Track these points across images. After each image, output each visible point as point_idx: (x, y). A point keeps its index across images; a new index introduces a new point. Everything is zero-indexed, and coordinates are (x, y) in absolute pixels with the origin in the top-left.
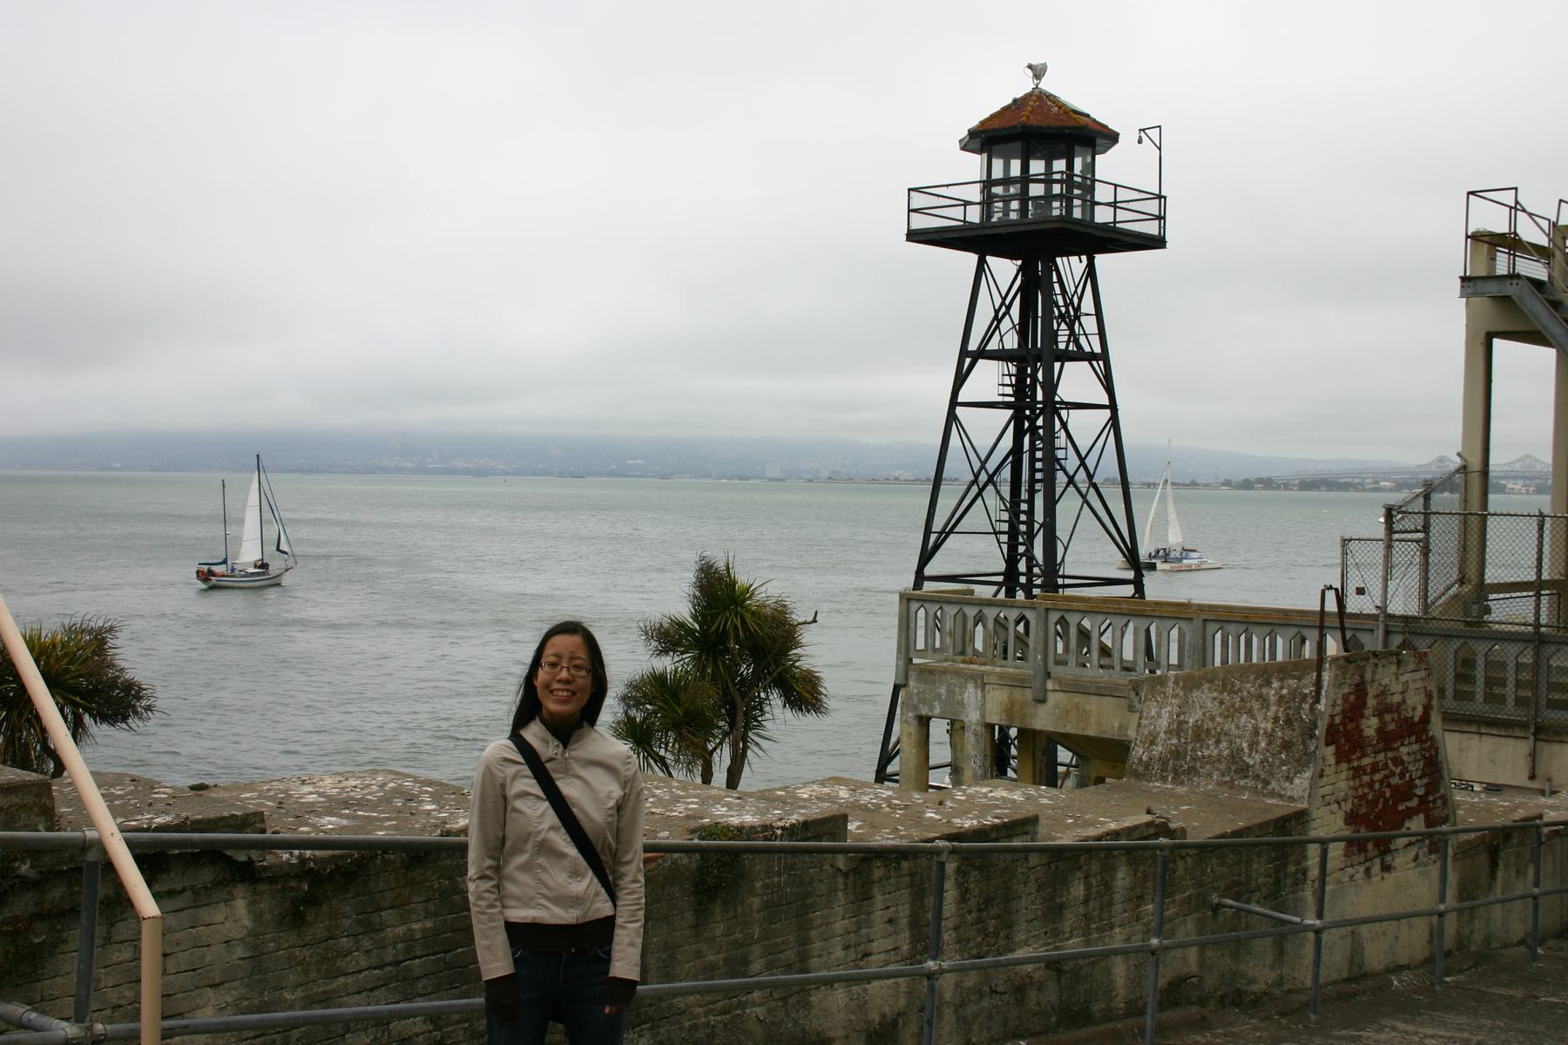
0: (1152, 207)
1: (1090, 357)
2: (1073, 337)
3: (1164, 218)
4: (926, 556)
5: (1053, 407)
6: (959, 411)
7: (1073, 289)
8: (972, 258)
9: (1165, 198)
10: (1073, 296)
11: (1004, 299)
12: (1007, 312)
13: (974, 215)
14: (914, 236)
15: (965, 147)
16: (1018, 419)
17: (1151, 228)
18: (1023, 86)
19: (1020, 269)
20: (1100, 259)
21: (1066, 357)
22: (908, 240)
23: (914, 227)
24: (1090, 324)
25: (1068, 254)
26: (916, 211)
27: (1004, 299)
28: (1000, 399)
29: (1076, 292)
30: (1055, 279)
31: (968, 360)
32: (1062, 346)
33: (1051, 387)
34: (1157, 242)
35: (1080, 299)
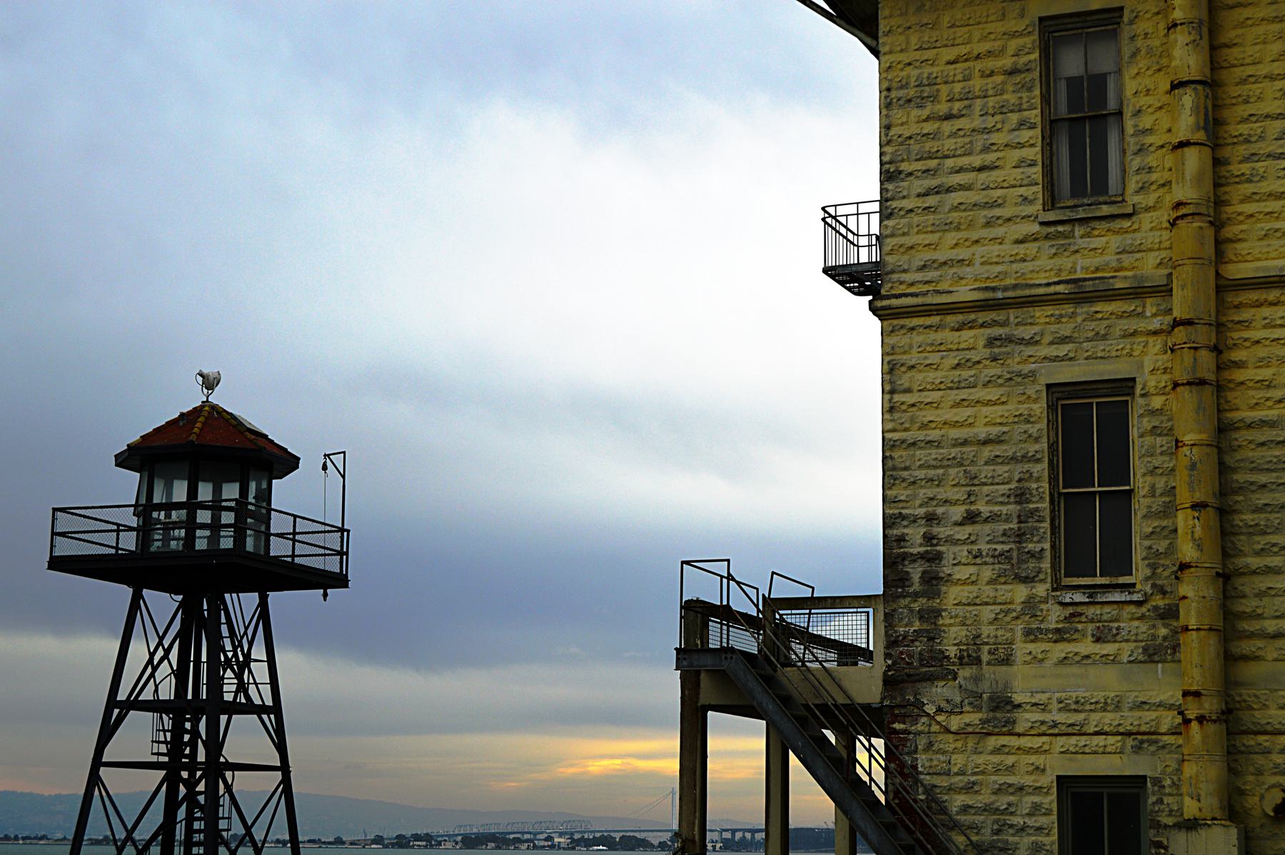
0: (333, 541)
1: (260, 710)
2: (242, 687)
3: (347, 554)
5: (217, 768)
6: (103, 772)
7: (242, 631)
8: (126, 592)
9: (348, 531)
10: (242, 638)
11: (161, 639)
12: (166, 656)
13: (129, 542)
14: (58, 563)
15: (124, 460)
16: (172, 780)
17: (332, 565)
18: (193, 398)
19: (182, 605)
20: (273, 597)
21: (234, 709)
22: (50, 568)
23: (56, 554)
24: (260, 671)
25: (238, 590)
26: (63, 534)
27: (161, 639)
28: (154, 759)
29: (246, 633)
30: (223, 620)
31: (116, 711)
32: (228, 697)
33: (215, 745)
34: (340, 580)
35: (251, 644)
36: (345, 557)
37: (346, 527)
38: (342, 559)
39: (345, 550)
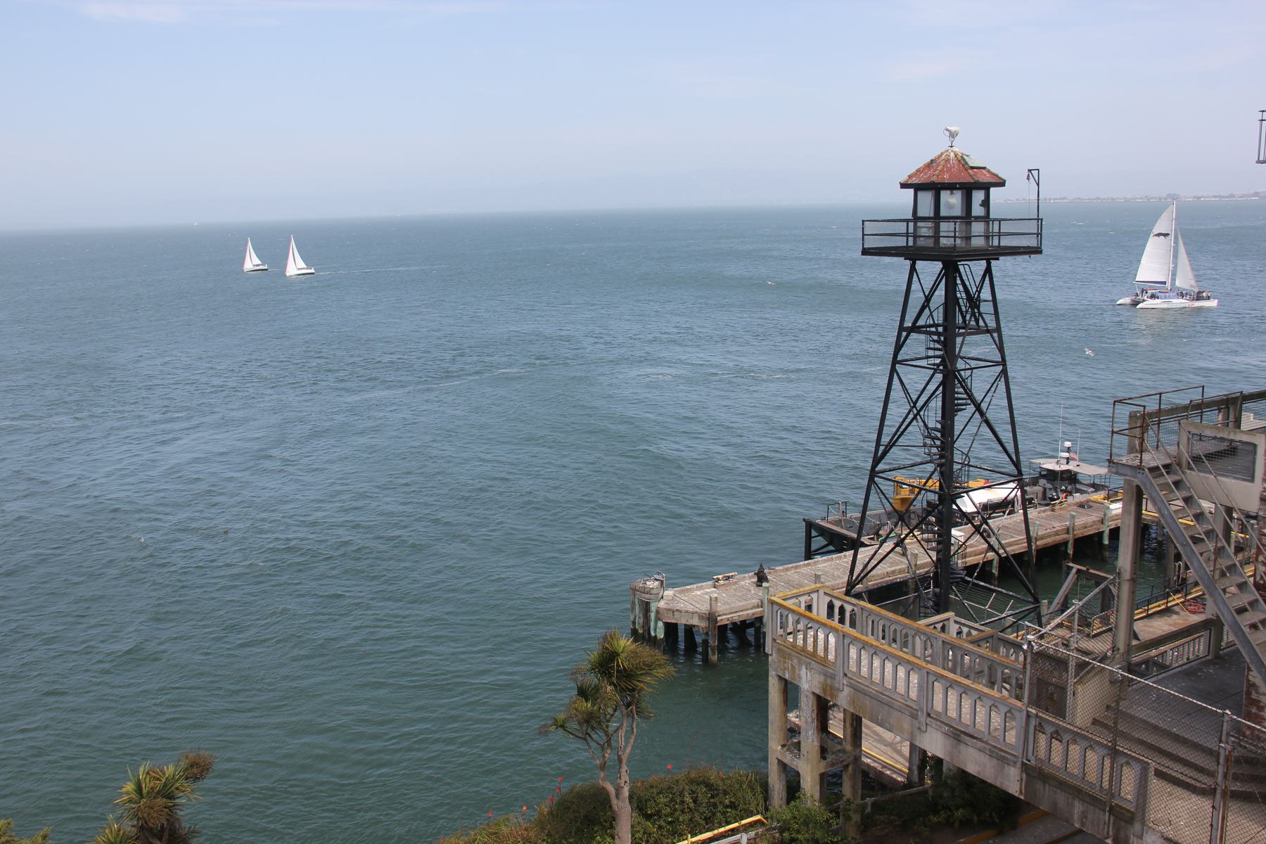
4: (877, 460)
9: (1042, 220)
14: (866, 252)
17: (1032, 242)
31: (904, 334)
34: (1037, 251)
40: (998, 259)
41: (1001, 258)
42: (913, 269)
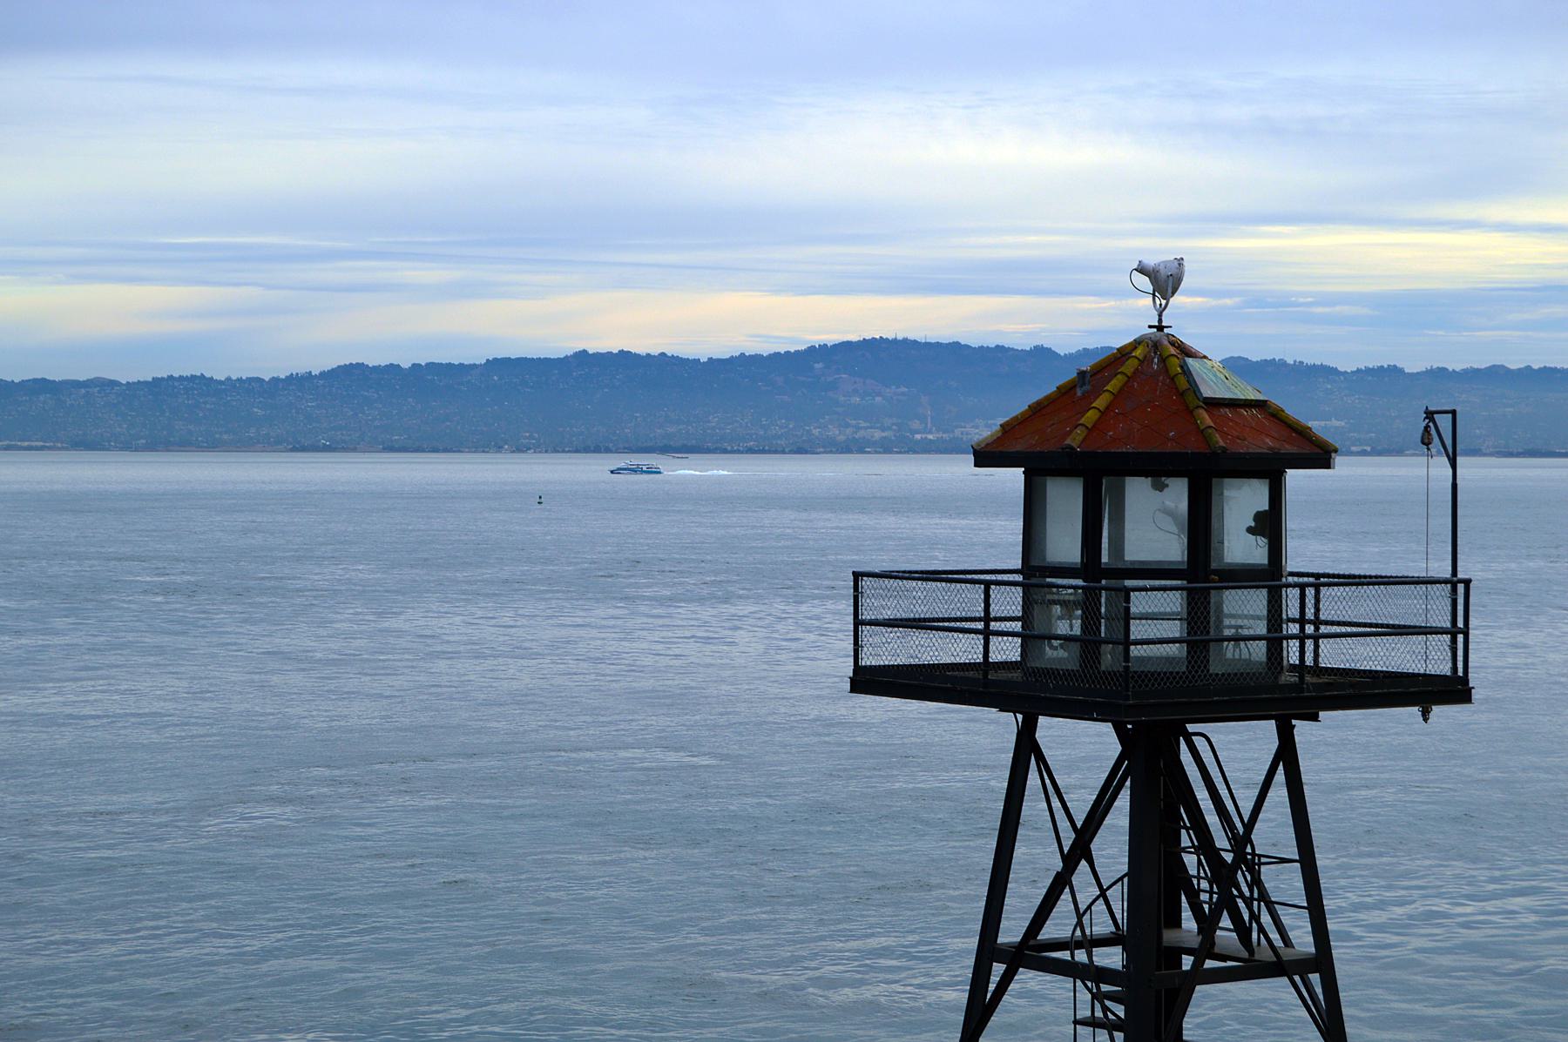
9: (1467, 582)
14: (868, 681)
23: (867, 660)
31: (998, 969)
34: (1454, 689)
36: (1460, 638)
37: (1460, 575)
38: (1454, 641)
39: (1460, 624)
40: (1315, 718)
41: (1321, 714)
42: (1027, 748)
